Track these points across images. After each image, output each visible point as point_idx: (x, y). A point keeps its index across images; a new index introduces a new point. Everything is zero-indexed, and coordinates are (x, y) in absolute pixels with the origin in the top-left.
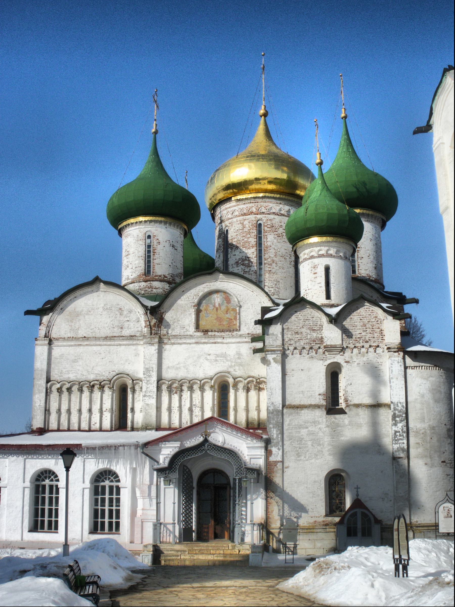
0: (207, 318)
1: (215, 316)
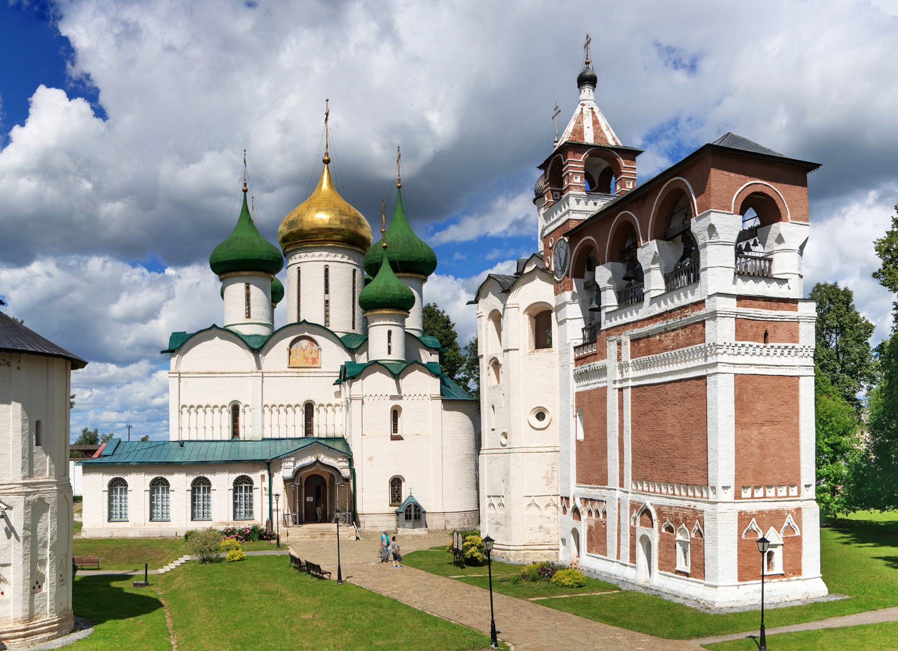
1: (303, 356)
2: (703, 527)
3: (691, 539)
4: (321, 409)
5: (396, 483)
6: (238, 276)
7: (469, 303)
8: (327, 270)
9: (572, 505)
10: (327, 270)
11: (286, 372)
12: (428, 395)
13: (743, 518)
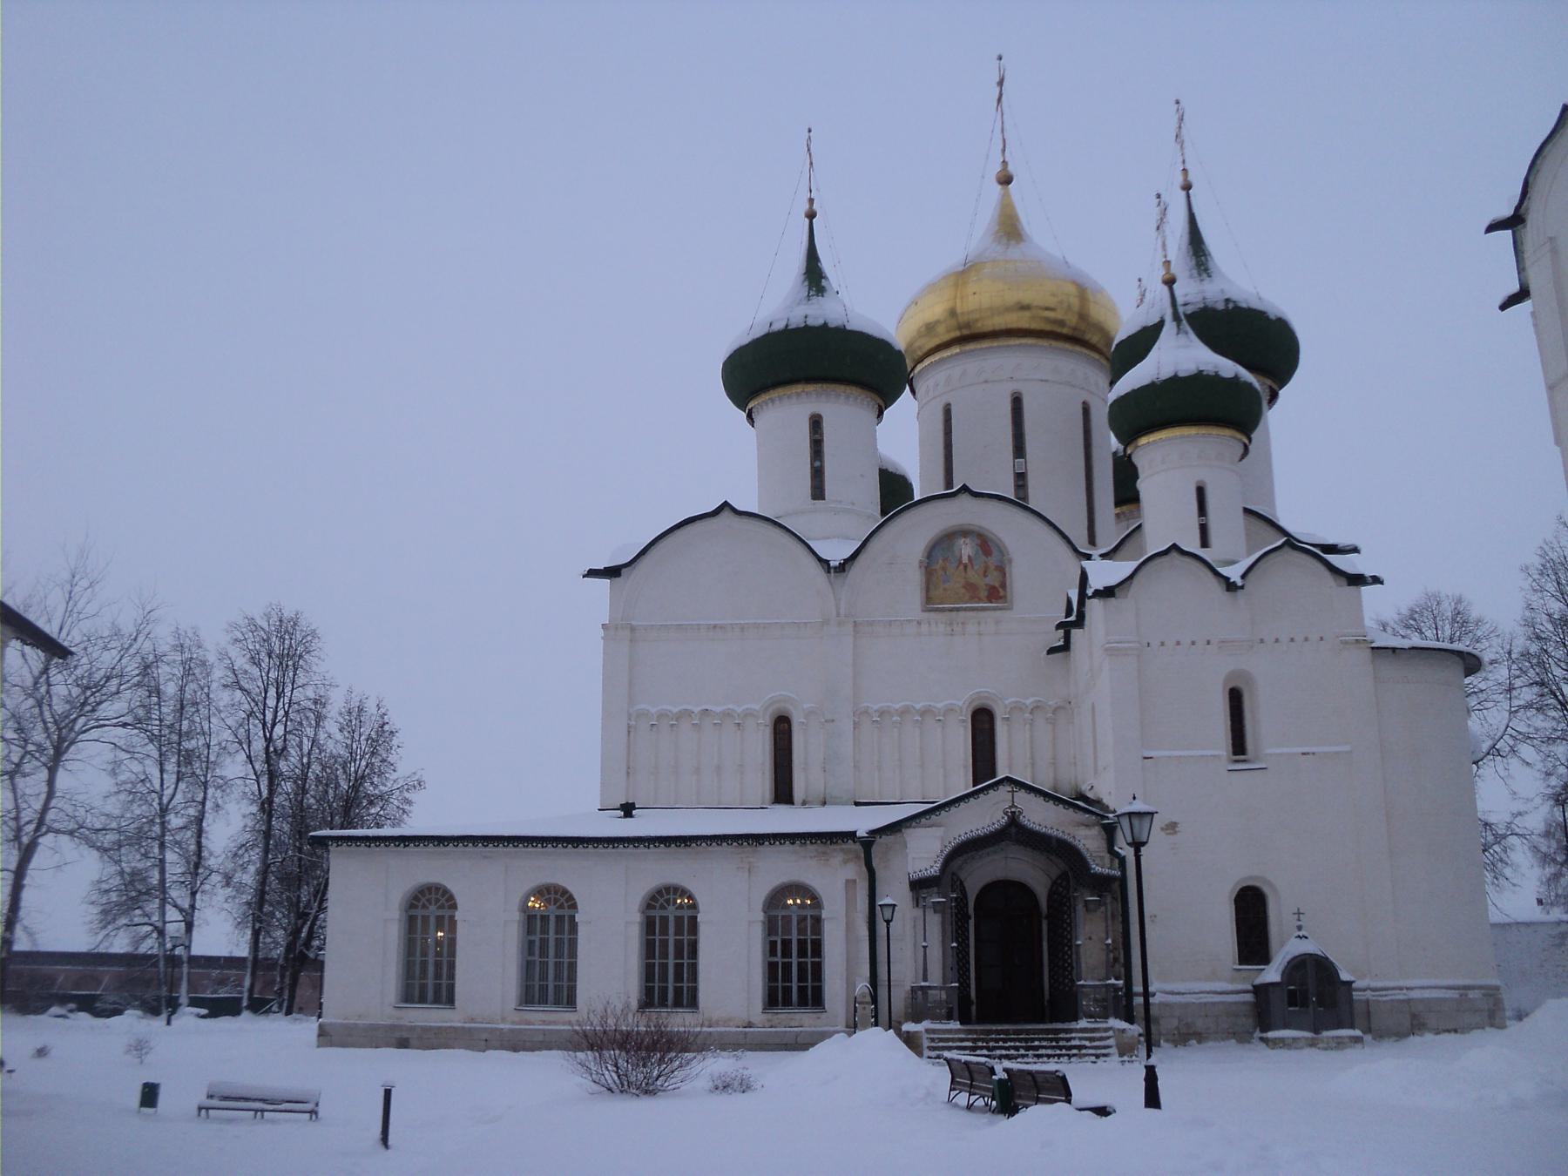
0: (947, 585)
8: (1017, 403)
10: (1017, 403)
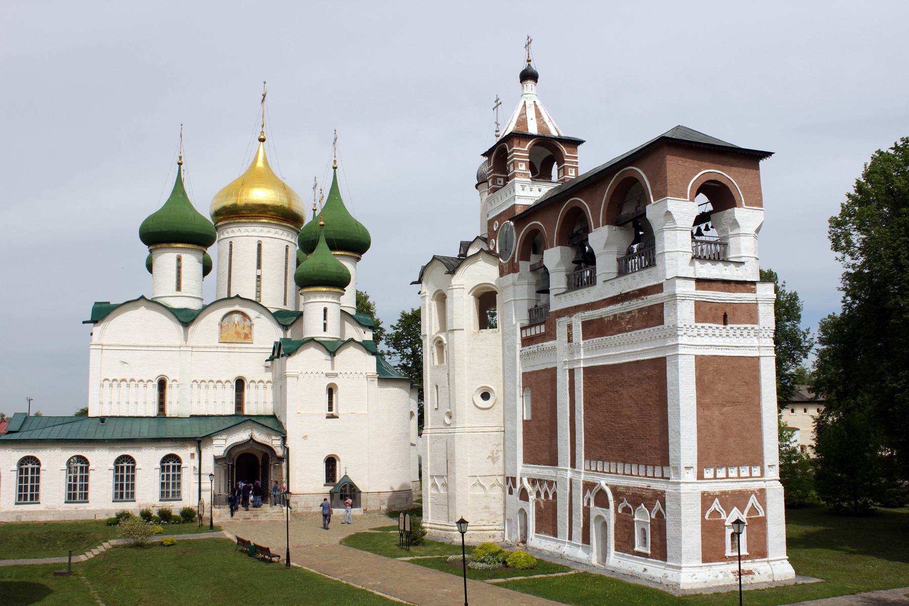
0: (228, 332)
2: (664, 506)
3: (651, 519)
4: (252, 385)
5: (331, 463)
6: (169, 248)
7: (413, 283)
8: (259, 245)
9: (518, 485)
10: (259, 245)
11: (217, 347)
12: (364, 373)
13: (707, 499)
